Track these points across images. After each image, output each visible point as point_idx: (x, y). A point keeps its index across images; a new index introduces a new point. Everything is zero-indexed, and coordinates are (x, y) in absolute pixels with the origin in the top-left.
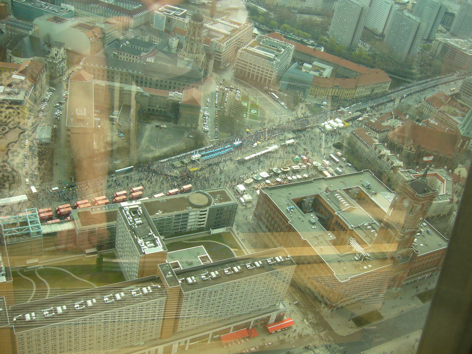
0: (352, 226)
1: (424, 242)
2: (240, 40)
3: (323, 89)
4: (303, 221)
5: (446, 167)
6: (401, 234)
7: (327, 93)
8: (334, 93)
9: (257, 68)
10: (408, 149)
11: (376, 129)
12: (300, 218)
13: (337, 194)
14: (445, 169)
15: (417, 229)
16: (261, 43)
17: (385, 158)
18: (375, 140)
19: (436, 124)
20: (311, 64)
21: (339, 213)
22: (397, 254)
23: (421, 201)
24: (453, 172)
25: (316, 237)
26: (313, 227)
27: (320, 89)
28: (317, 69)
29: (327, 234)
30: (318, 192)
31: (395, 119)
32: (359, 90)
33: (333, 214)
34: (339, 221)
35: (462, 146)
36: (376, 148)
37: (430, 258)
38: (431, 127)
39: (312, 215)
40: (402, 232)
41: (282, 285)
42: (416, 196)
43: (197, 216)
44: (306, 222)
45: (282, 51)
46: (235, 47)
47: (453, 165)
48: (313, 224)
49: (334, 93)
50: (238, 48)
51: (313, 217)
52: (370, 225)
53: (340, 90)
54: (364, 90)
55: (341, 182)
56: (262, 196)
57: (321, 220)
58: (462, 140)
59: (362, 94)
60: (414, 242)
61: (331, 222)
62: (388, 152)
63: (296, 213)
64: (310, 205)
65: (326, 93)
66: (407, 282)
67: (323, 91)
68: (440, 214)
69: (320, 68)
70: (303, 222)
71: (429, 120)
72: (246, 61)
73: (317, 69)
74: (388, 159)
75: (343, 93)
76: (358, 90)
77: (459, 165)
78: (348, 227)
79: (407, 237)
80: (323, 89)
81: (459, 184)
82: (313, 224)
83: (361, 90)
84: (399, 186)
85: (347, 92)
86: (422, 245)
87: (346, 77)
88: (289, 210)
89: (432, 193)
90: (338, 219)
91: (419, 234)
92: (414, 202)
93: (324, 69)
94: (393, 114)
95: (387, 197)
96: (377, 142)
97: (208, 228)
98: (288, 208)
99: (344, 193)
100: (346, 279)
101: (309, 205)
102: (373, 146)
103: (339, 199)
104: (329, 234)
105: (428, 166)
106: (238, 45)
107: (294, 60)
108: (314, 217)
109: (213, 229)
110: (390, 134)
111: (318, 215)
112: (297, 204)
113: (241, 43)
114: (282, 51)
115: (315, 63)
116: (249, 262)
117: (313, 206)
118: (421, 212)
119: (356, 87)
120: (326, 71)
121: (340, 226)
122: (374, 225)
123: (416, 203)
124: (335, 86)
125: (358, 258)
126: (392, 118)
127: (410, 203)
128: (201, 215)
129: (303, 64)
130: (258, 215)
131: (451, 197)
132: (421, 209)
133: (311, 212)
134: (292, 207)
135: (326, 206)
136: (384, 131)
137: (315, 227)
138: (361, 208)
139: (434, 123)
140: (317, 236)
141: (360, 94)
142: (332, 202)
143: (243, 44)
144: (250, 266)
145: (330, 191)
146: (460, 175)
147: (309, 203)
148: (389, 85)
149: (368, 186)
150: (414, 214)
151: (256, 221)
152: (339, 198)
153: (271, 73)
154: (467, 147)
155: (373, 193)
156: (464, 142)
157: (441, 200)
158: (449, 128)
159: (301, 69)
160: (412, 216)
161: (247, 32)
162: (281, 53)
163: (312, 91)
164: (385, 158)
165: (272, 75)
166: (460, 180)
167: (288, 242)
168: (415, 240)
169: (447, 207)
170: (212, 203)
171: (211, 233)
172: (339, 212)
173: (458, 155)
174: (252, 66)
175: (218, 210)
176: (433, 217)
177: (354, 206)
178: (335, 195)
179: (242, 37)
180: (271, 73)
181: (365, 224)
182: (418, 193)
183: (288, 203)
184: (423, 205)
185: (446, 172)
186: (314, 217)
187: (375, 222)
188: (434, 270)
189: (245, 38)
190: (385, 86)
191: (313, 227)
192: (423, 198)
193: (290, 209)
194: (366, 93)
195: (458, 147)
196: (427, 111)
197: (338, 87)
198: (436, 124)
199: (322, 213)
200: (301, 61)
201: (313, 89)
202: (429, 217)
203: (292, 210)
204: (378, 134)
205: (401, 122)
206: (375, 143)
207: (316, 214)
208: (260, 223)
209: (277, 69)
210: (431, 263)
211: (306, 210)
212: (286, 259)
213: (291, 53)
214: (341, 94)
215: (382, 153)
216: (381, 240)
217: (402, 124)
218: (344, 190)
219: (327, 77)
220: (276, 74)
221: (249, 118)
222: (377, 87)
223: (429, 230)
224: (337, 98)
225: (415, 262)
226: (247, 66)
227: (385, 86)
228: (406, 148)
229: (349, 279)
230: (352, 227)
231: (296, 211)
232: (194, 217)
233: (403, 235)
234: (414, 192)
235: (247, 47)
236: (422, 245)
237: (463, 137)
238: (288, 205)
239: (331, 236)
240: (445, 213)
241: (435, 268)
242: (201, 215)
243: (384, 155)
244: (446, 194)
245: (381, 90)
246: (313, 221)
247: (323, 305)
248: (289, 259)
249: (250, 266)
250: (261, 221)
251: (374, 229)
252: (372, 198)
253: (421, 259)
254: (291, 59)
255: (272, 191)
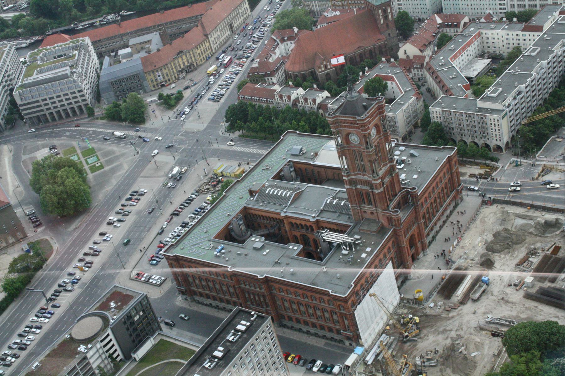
0: (313, 215)
1: (417, 171)
2: (6, 78)
3: (165, 69)
4: (246, 255)
5: (383, 59)
6: (377, 182)
7: (174, 70)
8: (184, 63)
9: (56, 100)
10: (323, 69)
11: (266, 73)
12: (240, 254)
13: (268, 190)
14: (385, 63)
15: (392, 160)
16: (39, 63)
17: (301, 100)
18: (274, 88)
19: (338, 13)
20: (127, 47)
21: (286, 212)
22: (390, 209)
23: (369, 123)
24: (396, 58)
25: (276, 263)
26: (265, 253)
27: (161, 70)
28: (140, 47)
29: (288, 249)
30: (242, 204)
31: (282, 43)
32: (213, 37)
33: (281, 218)
34: (294, 221)
35: (386, 18)
36: (281, 97)
37: (437, 186)
38: (331, 23)
39: (253, 239)
40: (377, 178)
41: (273, 356)
42: (358, 120)
43: (101, 351)
44: (252, 254)
45: (75, 55)
46: (6, 91)
47: (392, 50)
48: (263, 248)
49: (184, 63)
50: (12, 90)
51: (256, 241)
52: (334, 198)
53: (188, 54)
54: (219, 33)
55: (263, 170)
56: (173, 262)
57: (268, 237)
58: (380, 12)
59: (221, 40)
60: (403, 180)
61: (285, 230)
62: (301, 91)
63: (230, 251)
64: (243, 227)
65: (172, 69)
66: (431, 236)
67: (167, 71)
68: (417, 123)
69: (143, 43)
70: (248, 257)
71: (326, 14)
72: (34, 100)
73: (140, 47)
74: (306, 100)
75: (194, 56)
76: (211, 39)
77: (400, 45)
78: (308, 221)
79: (387, 180)
80: (165, 69)
81: (414, 68)
82: (263, 248)
83: (216, 36)
84: (331, 124)
85: (199, 51)
86: (415, 177)
87: (186, 32)
88: (218, 254)
89: (376, 104)
90: (290, 220)
91: (403, 165)
92: (362, 131)
93: (149, 42)
94: (275, 38)
95: (333, 149)
96: (277, 88)
97: (128, 357)
98: (215, 253)
99: (276, 182)
100: (350, 288)
101: (241, 229)
102: (277, 97)
103: (275, 193)
104: (291, 247)
105: (361, 74)
106: (8, 85)
107: (101, 56)
108: (257, 240)
109: (134, 353)
110: (288, 66)
111: (262, 233)
112: (226, 240)
113: (11, 80)
114: (75, 55)
115: (132, 41)
116: (205, 360)
117: (248, 226)
118: (380, 137)
119: (206, 36)
120: (153, 42)
121: (300, 226)
122: (339, 195)
123: (366, 130)
124: (178, 54)
125: (347, 250)
126: (278, 44)
127: (358, 134)
128: (105, 346)
129: (117, 53)
130: (186, 291)
131: (414, 93)
132: (378, 132)
133: (251, 235)
134: (220, 248)
135: (264, 214)
136: (278, 69)
137: (268, 251)
138: (310, 185)
139: (334, 13)
140: (277, 260)
141: (218, 43)
142: (269, 205)
143: (16, 80)
144: (209, 364)
145: (256, 192)
146: (408, 57)
147: (240, 225)
148: (247, 5)
149: (301, 151)
150: (373, 145)
151: (189, 299)
152: (274, 192)
153: (81, 94)
154: (392, 14)
155: (312, 155)
156: (385, 12)
157: (403, 104)
158: (357, 7)
159: (120, 62)
160: (373, 150)
161: (8, 60)
162: (76, 58)
163: (152, 80)
164: (301, 100)
165: (83, 96)
166: (413, 63)
167: (247, 296)
168: (403, 176)
169: (418, 107)
170: (110, 318)
171: (137, 359)
172: (285, 210)
173: (389, 34)
174: (48, 101)
175: (125, 323)
176: (410, 133)
177: (299, 189)
178: (267, 192)
179: (6, 71)
180: (81, 94)
181: (328, 202)
182: (359, 116)
183: (212, 245)
184: (376, 126)
185: (388, 65)
186: (257, 240)
187: (338, 189)
188: (455, 198)
189: (12, 71)
190: (243, 9)
191: (265, 253)
192: (368, 117)
193: (220, 251)
194: (225, 36)
195: (382, 22)
196: (316, 6)
197: (181, 52)
198: (338, 13)
199: (266, 227)
200: (113, 51)
201: (152, 77)
202: (406, 134)
203: (223, 251)
204: (273, 78)
205: (293, 42)
206: (275, 90)
207: (259, 234)
208: (197, 298)
209: (85, 82)
210: (443, 190)
211: (242, 239)
212: (252, 319)
213: (90, 49)
214: (193, 59)
215: (293, 97)
216: (360, 207)
217: (294, 43)
218: (273, 178)
219: (158, 50)
220: (89, 91)
221: (92, 173)
222: (234, 17)
223: (412, 151)
224: (192, 67)
225: (422, 203)
226: (40, 106)
227: (243, 9)
228: (320, 70)
229: (353, 285)
230: (314, 217)
231: (229, 248)
232: (97, 355)
233: (380, 180)
234: (353, 118)
235: (22, 82)
236: (415, 177)
237: (379, 7)
238: (214, 248)
239: (295, 248)
240: (420, 117)
241: (454, 193)
242: (105, 346)
243: (298, 98)
244: (405, 92)
245: (242, 18)
246: (259, 245)
247: (347, 343)
248: (255, 316)
249: (209, 364)
250: (197, 295)
251: (341, 199)
252: (316, 163)
253: (426, 195)
254: (96, 58)
255: (181, 246)
